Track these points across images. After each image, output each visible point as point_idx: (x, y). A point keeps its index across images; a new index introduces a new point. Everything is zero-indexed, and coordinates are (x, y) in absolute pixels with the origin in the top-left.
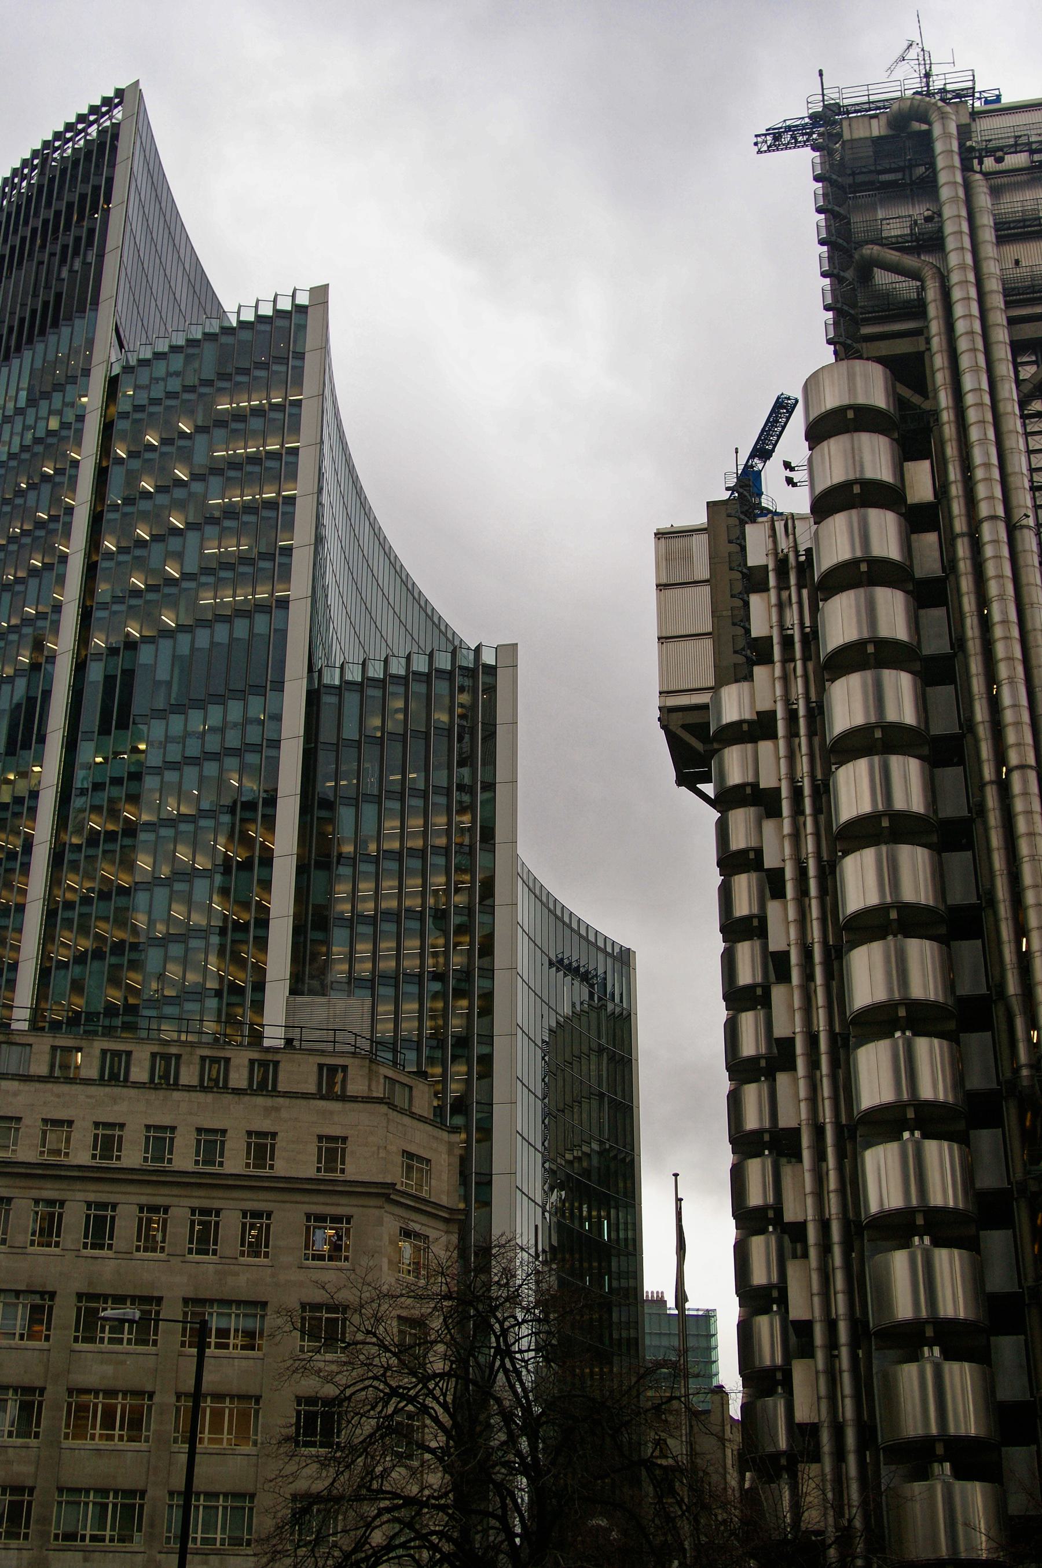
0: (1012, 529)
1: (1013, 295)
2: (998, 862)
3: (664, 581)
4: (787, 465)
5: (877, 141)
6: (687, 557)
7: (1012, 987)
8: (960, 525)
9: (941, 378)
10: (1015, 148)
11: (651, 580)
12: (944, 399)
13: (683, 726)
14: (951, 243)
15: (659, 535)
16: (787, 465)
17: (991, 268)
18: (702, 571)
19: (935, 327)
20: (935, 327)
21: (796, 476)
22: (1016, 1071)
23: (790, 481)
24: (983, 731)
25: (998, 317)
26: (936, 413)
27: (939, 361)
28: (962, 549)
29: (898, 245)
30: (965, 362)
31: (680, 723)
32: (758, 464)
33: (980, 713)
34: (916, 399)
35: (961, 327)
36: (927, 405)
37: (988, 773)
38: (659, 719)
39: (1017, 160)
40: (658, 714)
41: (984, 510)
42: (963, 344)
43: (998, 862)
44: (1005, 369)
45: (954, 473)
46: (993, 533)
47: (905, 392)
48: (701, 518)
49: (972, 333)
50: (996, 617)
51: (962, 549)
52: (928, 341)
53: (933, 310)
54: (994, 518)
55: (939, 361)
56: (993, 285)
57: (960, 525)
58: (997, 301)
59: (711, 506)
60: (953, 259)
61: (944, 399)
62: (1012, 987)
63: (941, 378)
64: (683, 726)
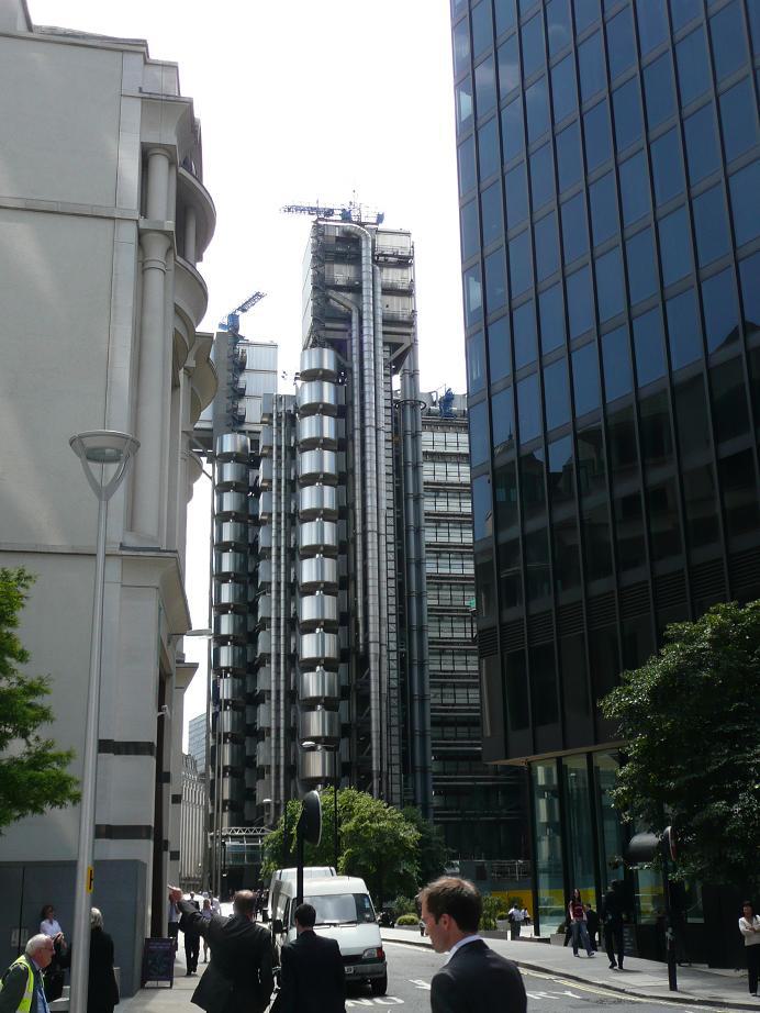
0: (377, 430)
1: (385, 322)
2: (359, 566)
5: (338, 239)
7: (360, 615)
8: (357, 425)
9: (355, 358)
10: (392, 256)
12: (356, 368)
13: (197, 438)
14: (364, 293)
17: (379, 312)
19: (355, 334)
20: (355, 334)
22: (358, 645)
24: (358, 513)
25: (380, 336)
26: (351, 370)
27: (355, 350)
28: (357, 435)
29: (339, 288)
30: (366, 355)
32: (239, 313)
33: (358, 505)
34: (343, 361)
35: (365, 339)
36: (347, 364)
37: (359, 529)
39: (390, 259)
41: (368, 422)
42: (366, 347)
43: (359, 566)
44: (380, 351)
45: (357, 401)
46: (370, 432)
47: (339, 357)
49: (369, 343)
50: (368, 469)
51: (357, 435)
52: (351, 335)
53: (355, 326)
54: (370, 426)
55: (355, 350)
56: (380, 320)
57: (357, 424)
58: (380, 328)
60: (365, 308)
61: (356, 368)
62: (360, 615)
63: (355, 358)
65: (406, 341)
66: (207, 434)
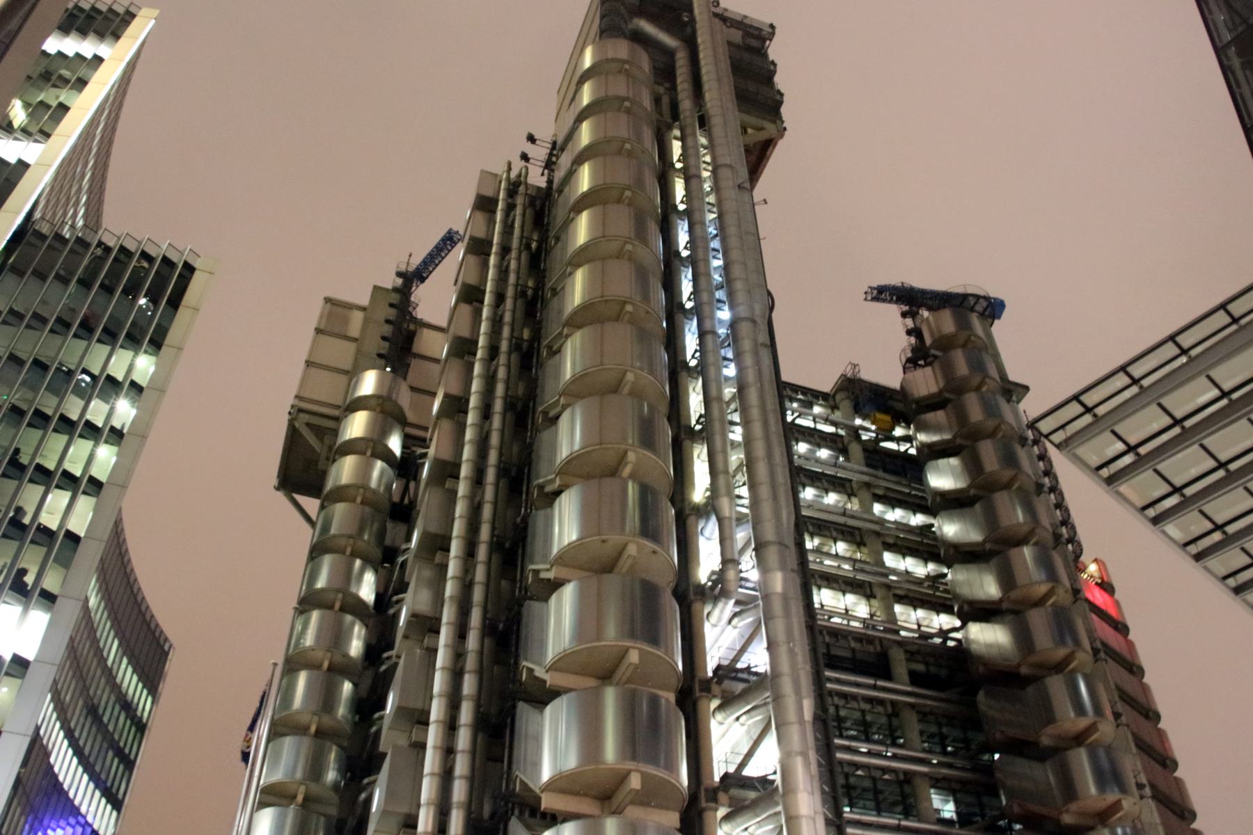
3: (322, 327)
4: (531, 139)
6: (346, 321)
11: (314, 324)
13: (308, 425)
15: (328, 300)
16: (531, 139)
18: (355, 328)
21: (531, 150)
23: (525, 157)
31: (305, 421)
38: (290, 413)
40: (289, 409)
48: (365, 300)
59: (376, 289)
64: (308, 425)
65: (771, 129)
66: (330, 424)
